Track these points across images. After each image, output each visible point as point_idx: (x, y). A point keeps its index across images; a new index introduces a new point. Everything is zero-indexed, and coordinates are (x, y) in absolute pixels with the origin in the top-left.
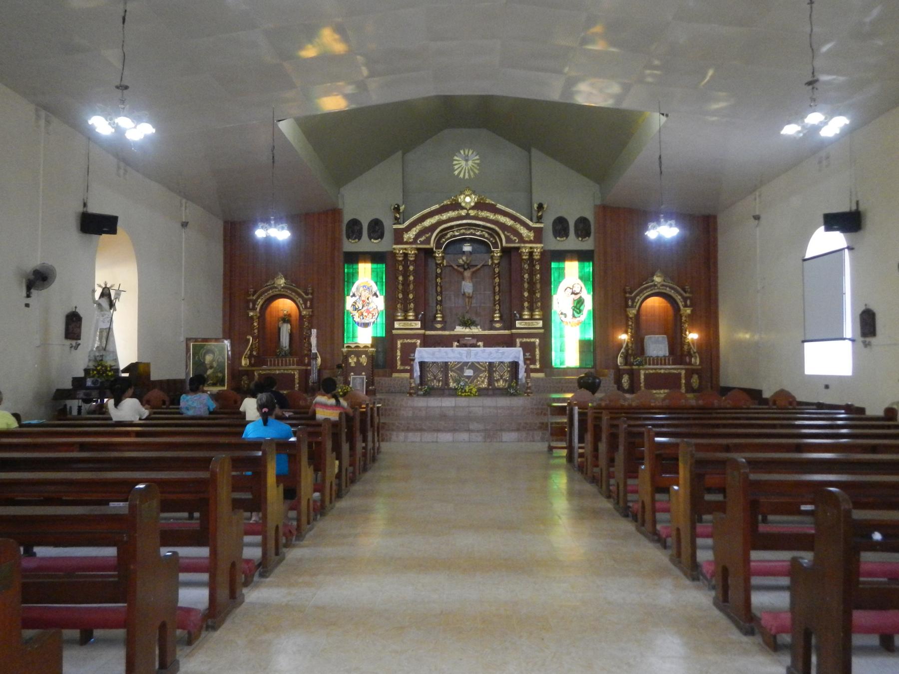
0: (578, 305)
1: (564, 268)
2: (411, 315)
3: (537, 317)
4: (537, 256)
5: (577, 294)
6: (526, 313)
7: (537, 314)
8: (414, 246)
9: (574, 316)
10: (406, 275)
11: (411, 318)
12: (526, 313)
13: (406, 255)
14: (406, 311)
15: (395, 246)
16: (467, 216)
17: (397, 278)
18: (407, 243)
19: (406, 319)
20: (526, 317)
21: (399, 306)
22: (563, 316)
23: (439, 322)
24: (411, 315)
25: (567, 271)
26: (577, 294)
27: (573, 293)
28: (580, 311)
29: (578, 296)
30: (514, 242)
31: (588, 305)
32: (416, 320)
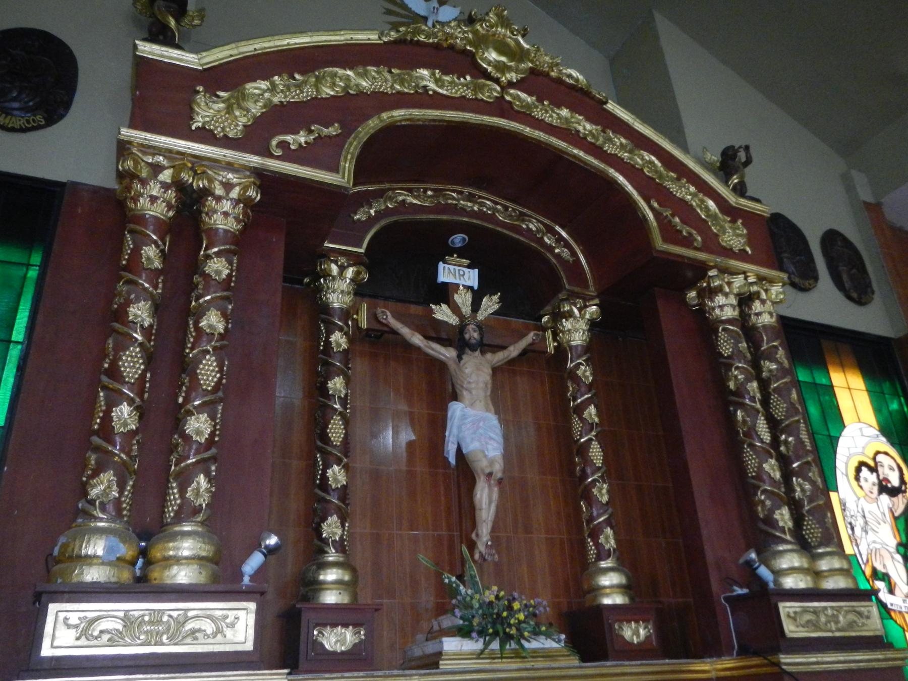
2: (185, 554)
4: (764, 316)
8: (255, 160)
10: (177, 312)
11: (183, 576)
13: (190, 203)
14: (147, 529)
15: (126, 133)
16: (501, 107)
17: (121, 315)
18: (205, 136)
19: (142, 584)
21: (103, 486)
23: (337, 617)
24: (185, 554)
30: (687, 242)
32: (222, 584)
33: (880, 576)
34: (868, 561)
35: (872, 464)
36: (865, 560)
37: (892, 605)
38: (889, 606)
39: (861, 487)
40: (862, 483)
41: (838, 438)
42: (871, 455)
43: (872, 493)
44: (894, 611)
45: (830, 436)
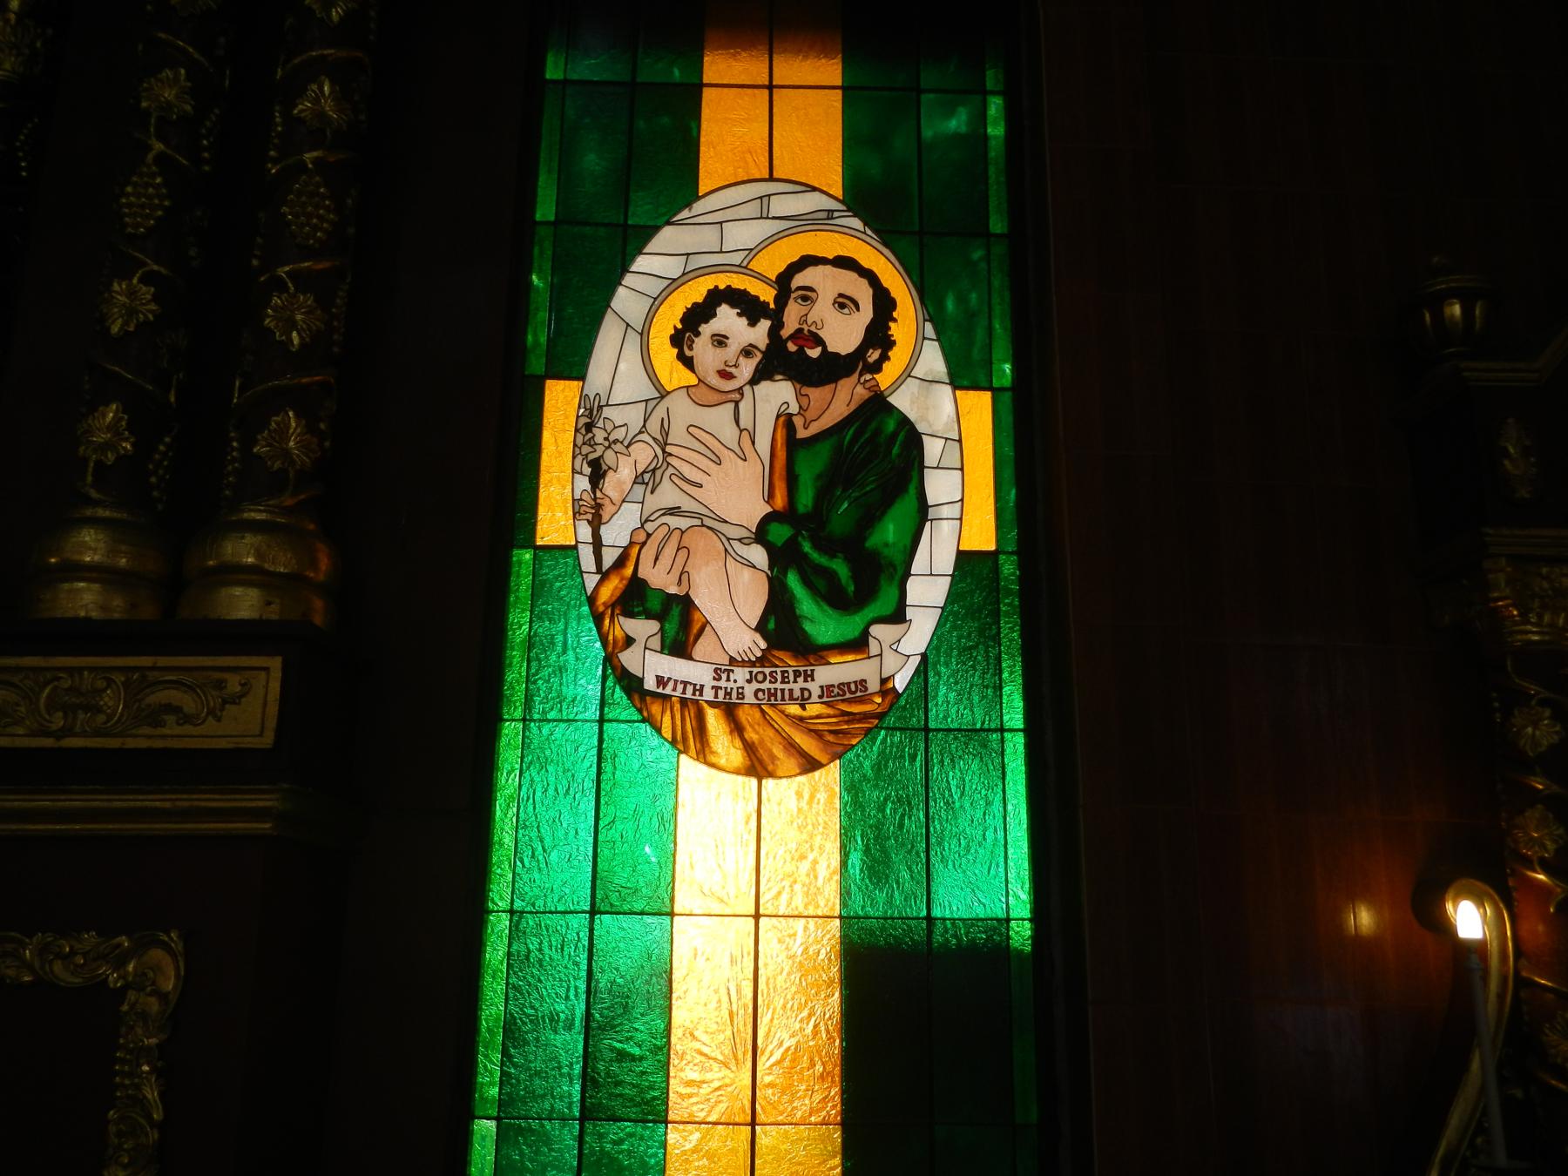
0: (840, 510)
1: (689, 98)
3: (244, 603)
5: (832, 368)
6: (90, 546)
7: (251, 570)
9: (781, 630)
12: (90, 546)
20: (85, 600)
22: (643, 628)
25: (728, 128)
26: (832, 368)
27: (778, 361)
28: (872, 583)
29: (842, 399)
31: (962, 503)
33: (654, 604)
34: (620, 562)
35: (767, 295)
36: (608, 562)
37: (661, 681)
38: (650, 684)
39: (688, 363)
40: (702, 348)
41: (650, 231)
42: (781, 267)
43: (725, 375)
44: (667, 697)
45: (625, 226)
